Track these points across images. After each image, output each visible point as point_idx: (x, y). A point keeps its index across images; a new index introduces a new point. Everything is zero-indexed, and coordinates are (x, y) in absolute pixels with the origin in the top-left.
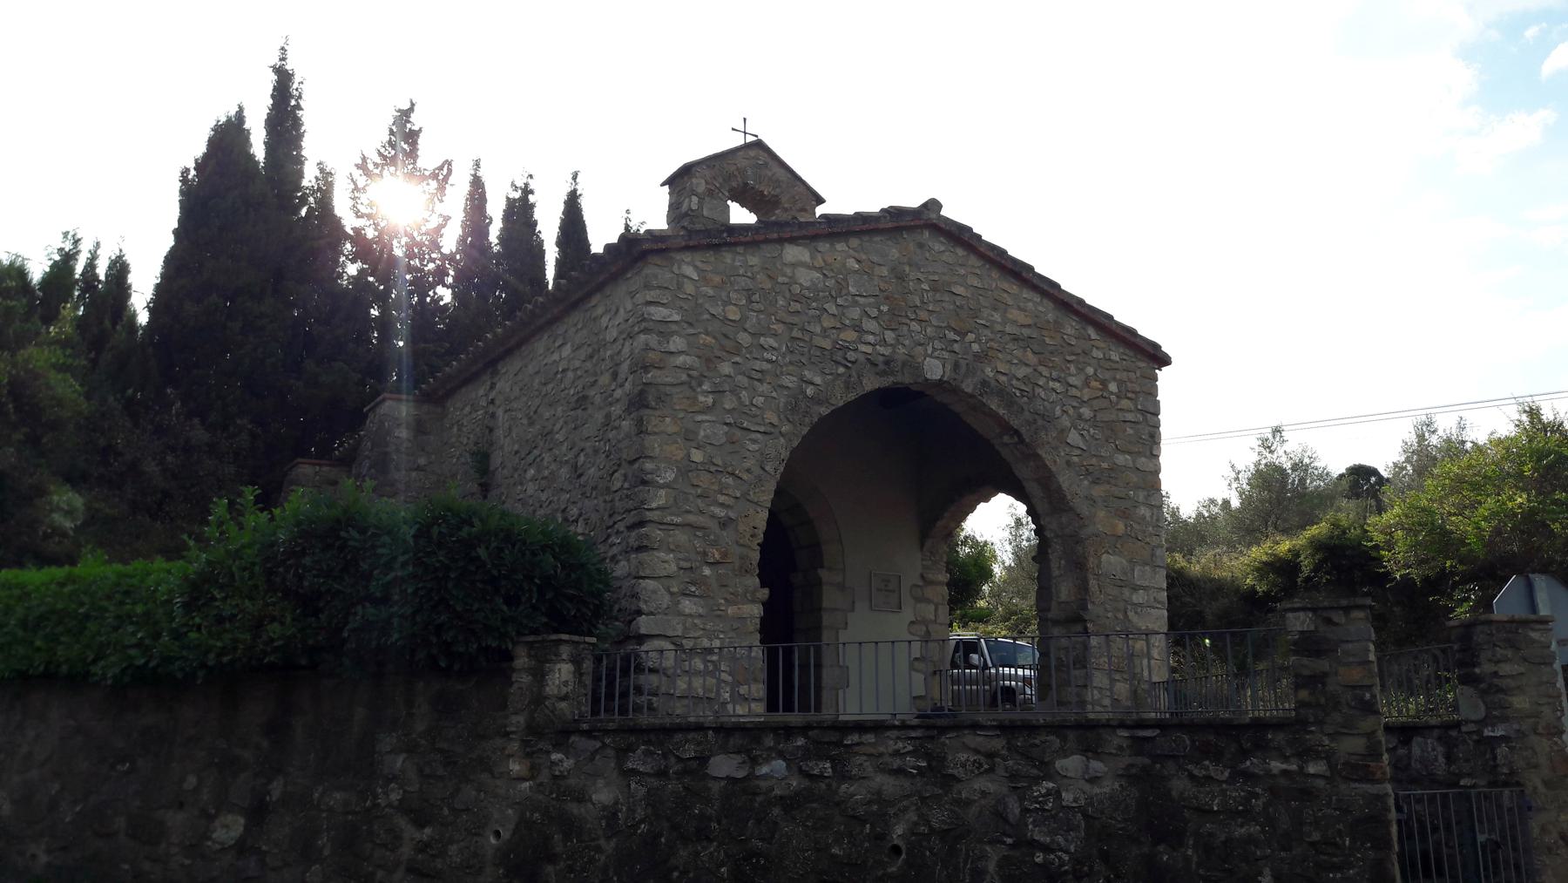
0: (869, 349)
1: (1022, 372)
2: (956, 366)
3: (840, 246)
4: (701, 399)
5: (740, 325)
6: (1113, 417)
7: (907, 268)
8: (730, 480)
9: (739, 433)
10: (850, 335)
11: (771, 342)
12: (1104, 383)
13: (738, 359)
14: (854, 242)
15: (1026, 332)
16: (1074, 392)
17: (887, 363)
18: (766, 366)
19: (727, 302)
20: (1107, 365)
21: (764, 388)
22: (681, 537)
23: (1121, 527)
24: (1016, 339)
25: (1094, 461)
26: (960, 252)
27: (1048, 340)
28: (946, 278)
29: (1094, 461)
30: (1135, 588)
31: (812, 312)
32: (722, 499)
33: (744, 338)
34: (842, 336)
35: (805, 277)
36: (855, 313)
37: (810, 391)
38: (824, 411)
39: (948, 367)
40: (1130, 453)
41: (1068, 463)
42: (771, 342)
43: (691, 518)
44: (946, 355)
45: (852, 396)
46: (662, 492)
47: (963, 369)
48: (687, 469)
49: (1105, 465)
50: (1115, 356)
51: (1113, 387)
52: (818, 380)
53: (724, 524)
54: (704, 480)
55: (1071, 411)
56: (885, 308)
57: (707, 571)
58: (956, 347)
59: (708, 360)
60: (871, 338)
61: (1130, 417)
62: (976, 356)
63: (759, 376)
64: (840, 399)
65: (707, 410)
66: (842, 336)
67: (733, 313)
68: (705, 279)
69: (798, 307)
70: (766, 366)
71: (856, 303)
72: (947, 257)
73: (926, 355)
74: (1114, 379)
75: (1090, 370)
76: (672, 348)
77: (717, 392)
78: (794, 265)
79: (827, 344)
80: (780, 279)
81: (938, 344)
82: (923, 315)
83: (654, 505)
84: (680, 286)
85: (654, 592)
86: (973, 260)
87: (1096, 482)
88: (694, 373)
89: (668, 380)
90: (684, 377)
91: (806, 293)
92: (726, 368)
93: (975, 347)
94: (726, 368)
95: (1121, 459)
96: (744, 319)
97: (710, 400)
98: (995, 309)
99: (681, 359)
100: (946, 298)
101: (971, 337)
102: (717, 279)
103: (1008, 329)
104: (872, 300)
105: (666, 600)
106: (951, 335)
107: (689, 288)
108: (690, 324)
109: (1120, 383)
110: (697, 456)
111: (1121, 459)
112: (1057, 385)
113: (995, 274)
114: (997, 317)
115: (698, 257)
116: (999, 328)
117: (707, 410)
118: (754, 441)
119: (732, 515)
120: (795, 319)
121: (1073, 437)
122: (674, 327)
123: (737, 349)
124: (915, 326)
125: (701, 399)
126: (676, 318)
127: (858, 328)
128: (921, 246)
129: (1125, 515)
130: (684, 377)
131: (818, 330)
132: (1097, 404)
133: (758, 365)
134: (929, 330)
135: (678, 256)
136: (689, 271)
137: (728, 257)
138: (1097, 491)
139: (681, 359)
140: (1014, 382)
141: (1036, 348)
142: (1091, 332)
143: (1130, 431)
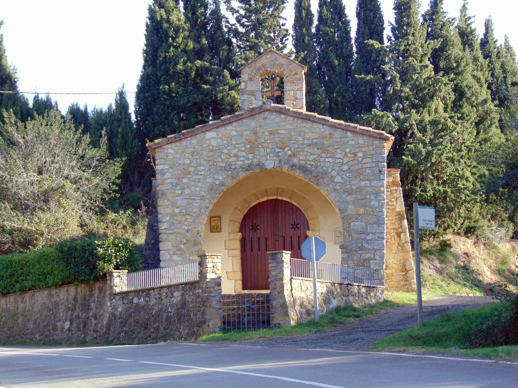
0: (241, 163)
1: (312, 158)
2: (280, 161)
3: (229, 127)
4: (177, 192)
5: (190, 165)
6: (360, 167)
7: (258, 129)
8: (189, 217)
9: (191, 201)
10: (233, 159)
11: (202, 168)
12: (355, 154)
13: (190, 176)
14: (235, 124)
15: (315, 141)
16: (339, 160)
17: (249, 166)
18: (200, 177)
19: (184, 159)
20: (358, 146)
21: (200, 185)
22: (172, 237)
23: (362, 211)
24: (309, 145)
25: (348, 186)
26: (283, 116)
27: (325, 142)
28: (277, 128)
29: (348, 186)
30: (368, 234)
31: (217, 155)
32: (186, 223)
33: (192, 169)
34: (230, 160)
35: (214, 143)
36: (235, 151)
37: (217, 183)
38: (224, 188)
39: (277, 163)
40: (368, 180)
41: (335, 189)
42: (202, 168)
43: (175, 231)
44: (275, 158)
45: (235, 181)
46: (165, 224)
47: (283, 162)
48: (173, 215)
49: (354, 187)
50: (361, 142)
51: (360, 155)
52: (220, 178)
53: (188, 231)
54: (180, 218)
55: (337, 169)
56: (248, 146)
57: (182, 246)
58: (280, 154)
59: (179, 179)
60: (242, 159)
61: (368, 165)
62: (290, 156)
63: (198, 180)
64: (230, 183)
65: (179, 195)
66: (230, 160)
67: (187, 162)
68: (176, 152)
69: (212, 153)
70: (200, 177)
71: (235, 147)
72: (278, 120)
73: (266, 160)
74: (361, 151)
75: (348, 150)
76: (166, 177)
77: (182, 189)
78: (210, 139)
79: (223, 165)
80: (204, 146)
81: (272, 155)
82: (265, 145)
83: (163, 228)
84: (167, 156)
85: (164, 254)
86: (289, 118)
87: (350, 194)
88: (174, 184)
89: (165, 188)
90: (170, 186)
91: (215, 148)
92: (185, 180)
93: (289, 153)
94: (185, 180)
95: (363, 184)
96: (191, 162)
97: (180, 192)
98: (300, 135)
99: (169, 181)
100: (277, 136)
101: (287, 149)
102: (180, 151)
103: (306, 142)
104: (242, 145)
105: (168, 257)
106: (278, 150)
107: (171, 157)
108: (172, 168)
109: (363, 152)
110: (177, 211)
111: (363, 184)
112: (330, 159)
113: (300, 121)
114: (300, 138)
115: (173, 145)
116: (301, 142)
117: (179, 195)
118: (197, 203)
119: (190, 228)
120: (211, 158)
121: (338, 179)
122: (166, 171)
123: (189, 173)
124: (262, 150)
125: (177, 192)
126: (167, 167)
127: (236, 156)
128: (265, 118)
129: (364, 206)
130: (170, 186)
131: (220, 160)
132: (351, 163)
133: (197, 177)
134: (268, 150)
135: (167, 146)
136: (171, 151)
137: (184, 142)
138: (349, 198)
139: (169, 181)
140: (308, 162)
141: (319, 146)
142: (349, 134)
143: (368, 171)
